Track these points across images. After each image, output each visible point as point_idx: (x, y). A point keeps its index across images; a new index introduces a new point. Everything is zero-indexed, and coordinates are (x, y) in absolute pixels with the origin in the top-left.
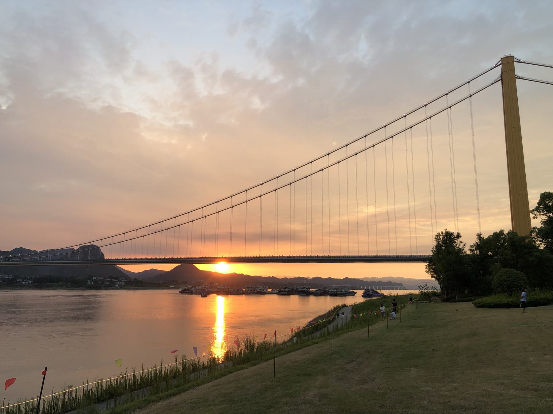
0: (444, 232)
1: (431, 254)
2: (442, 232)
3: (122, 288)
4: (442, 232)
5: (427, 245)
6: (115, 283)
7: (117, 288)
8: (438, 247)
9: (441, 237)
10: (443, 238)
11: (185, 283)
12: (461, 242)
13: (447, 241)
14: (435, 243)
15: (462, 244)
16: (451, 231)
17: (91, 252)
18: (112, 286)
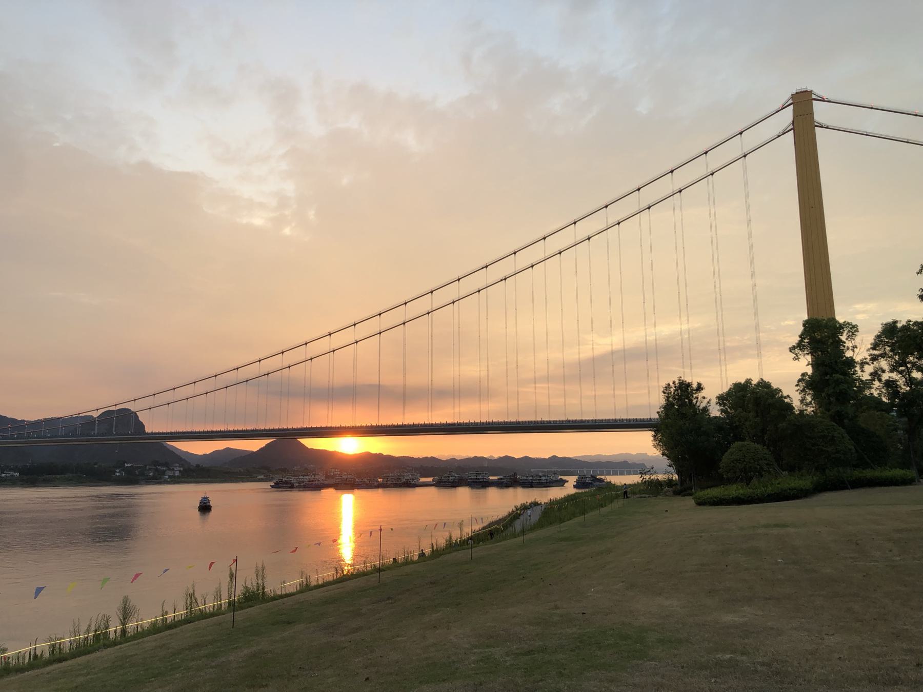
0: (677, 382)
1: (657, 416)
2: (674, 382)
3: (174, 480)
4: (674, 382)
5: (651, 403)
6: (163, 473)
7: (166, 482)
8: (668, 407)
9: (672, 390)
10: (675, 391)
11: (284, 470)
12: (704, 398)
13: (682, 396)
14: (663, 402)
15: (705, 401)
16: (688, 380)
17: (121, 421)
18: (157, 479)
